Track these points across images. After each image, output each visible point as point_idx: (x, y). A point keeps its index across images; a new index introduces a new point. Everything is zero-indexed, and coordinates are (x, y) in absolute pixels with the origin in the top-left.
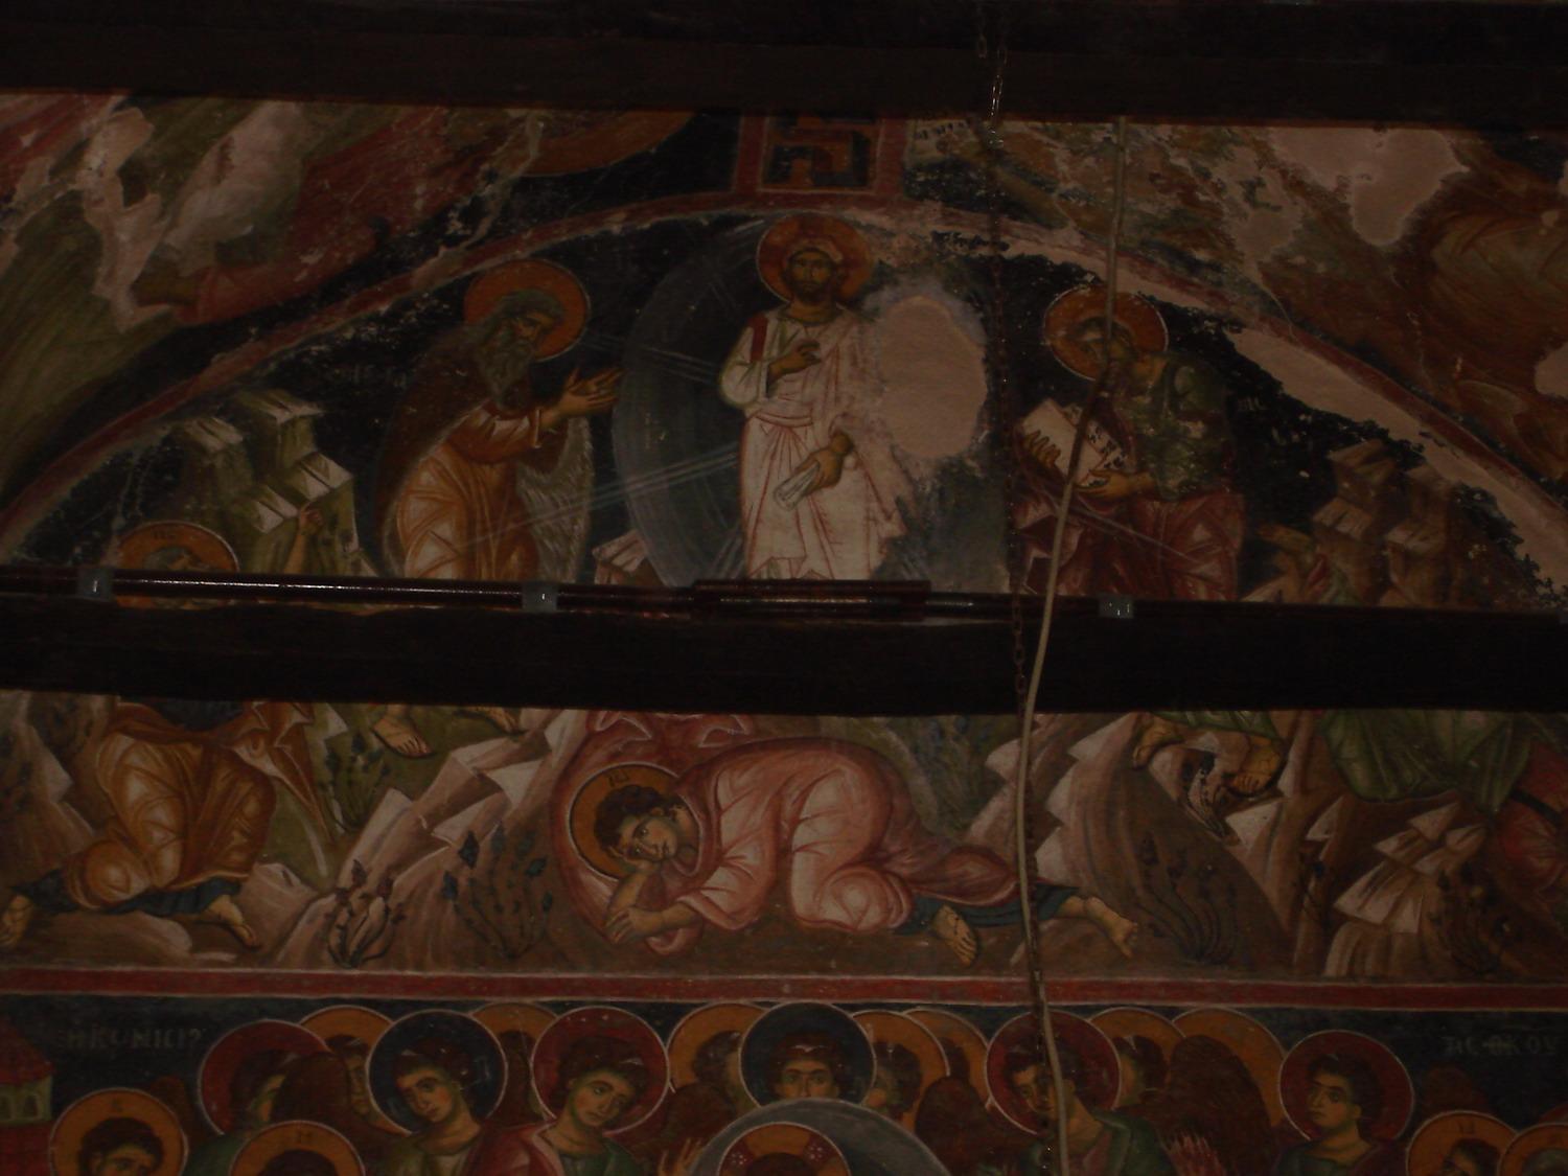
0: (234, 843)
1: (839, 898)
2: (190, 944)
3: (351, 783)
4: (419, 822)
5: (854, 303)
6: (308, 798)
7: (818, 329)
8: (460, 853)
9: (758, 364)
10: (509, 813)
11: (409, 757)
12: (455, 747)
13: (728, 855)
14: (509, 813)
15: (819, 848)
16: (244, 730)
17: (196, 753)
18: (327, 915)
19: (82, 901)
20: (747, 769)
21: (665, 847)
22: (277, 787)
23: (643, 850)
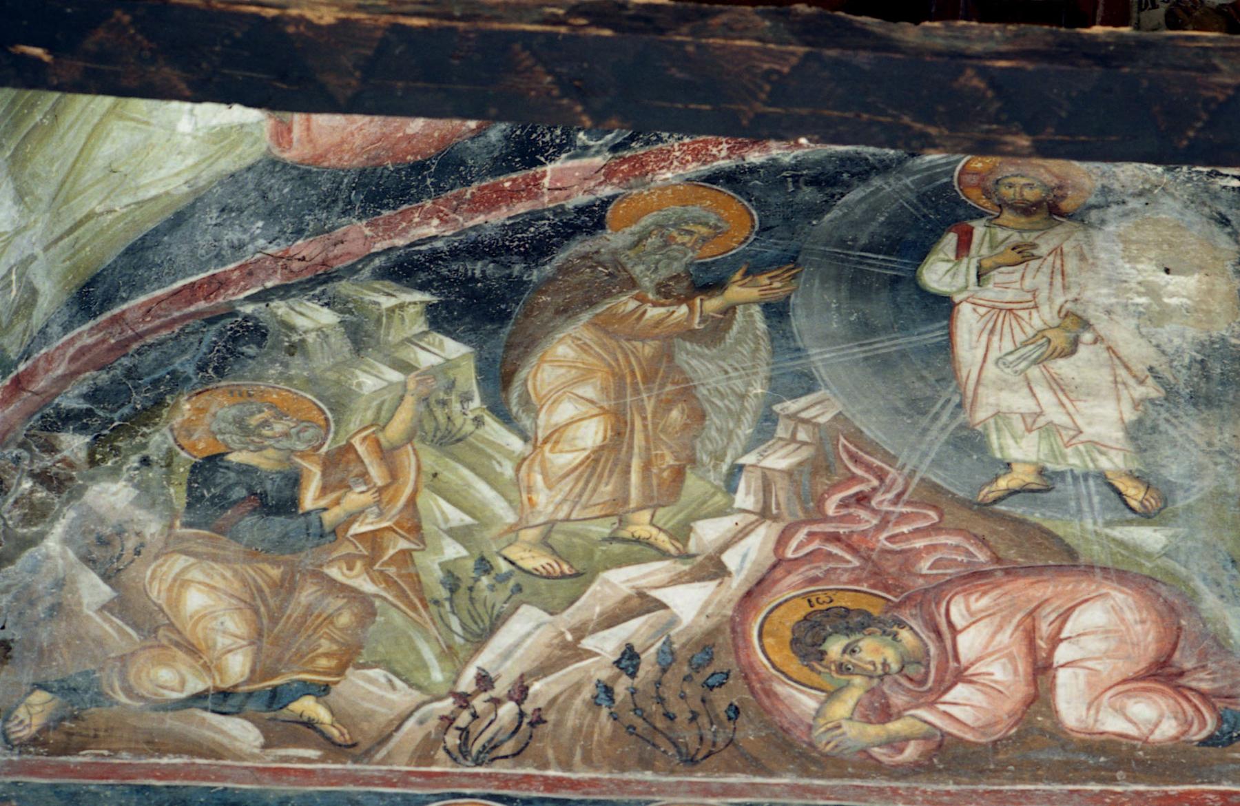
0: (320, 651)
1: (1122, 712)
2: (262, 740)
3: (472, 599)
4: (562, 633)
5: (1078, 216)
6: (415, 609)
7: (1035, 234)
8: (617, 663)
9: (965, 260)
10: (677, 630)
11: (549, 577)
12: (607, 569)
13: (970, 671)
14: (677, 630)
15: (1090, 664)
16: (335, 555)
17: (276, 573)
18: (442, 718)
19: (123, 698)
20: (985, 593)
21: (885, 664)
22: (377, 603)
23: (855, 666)
